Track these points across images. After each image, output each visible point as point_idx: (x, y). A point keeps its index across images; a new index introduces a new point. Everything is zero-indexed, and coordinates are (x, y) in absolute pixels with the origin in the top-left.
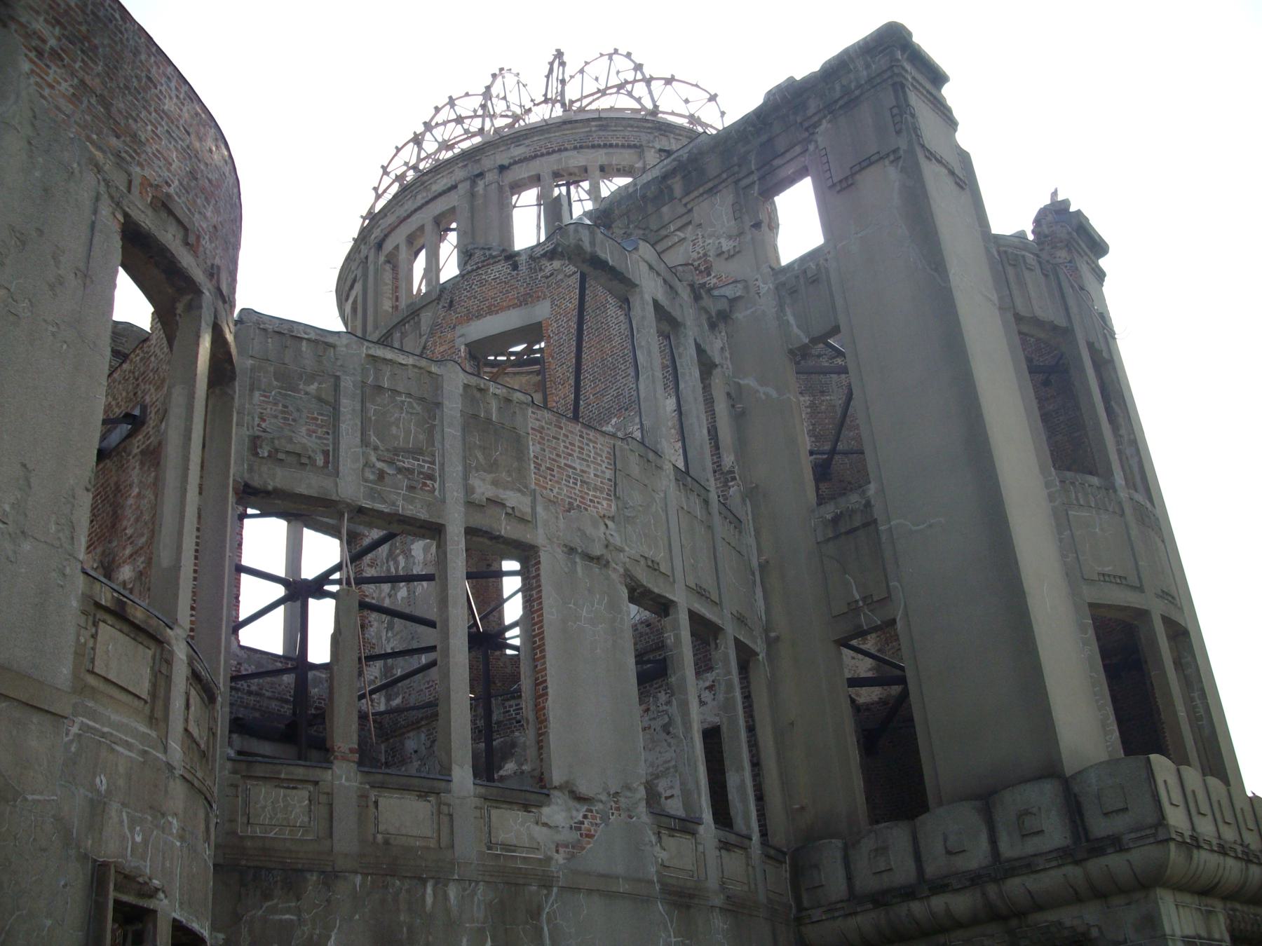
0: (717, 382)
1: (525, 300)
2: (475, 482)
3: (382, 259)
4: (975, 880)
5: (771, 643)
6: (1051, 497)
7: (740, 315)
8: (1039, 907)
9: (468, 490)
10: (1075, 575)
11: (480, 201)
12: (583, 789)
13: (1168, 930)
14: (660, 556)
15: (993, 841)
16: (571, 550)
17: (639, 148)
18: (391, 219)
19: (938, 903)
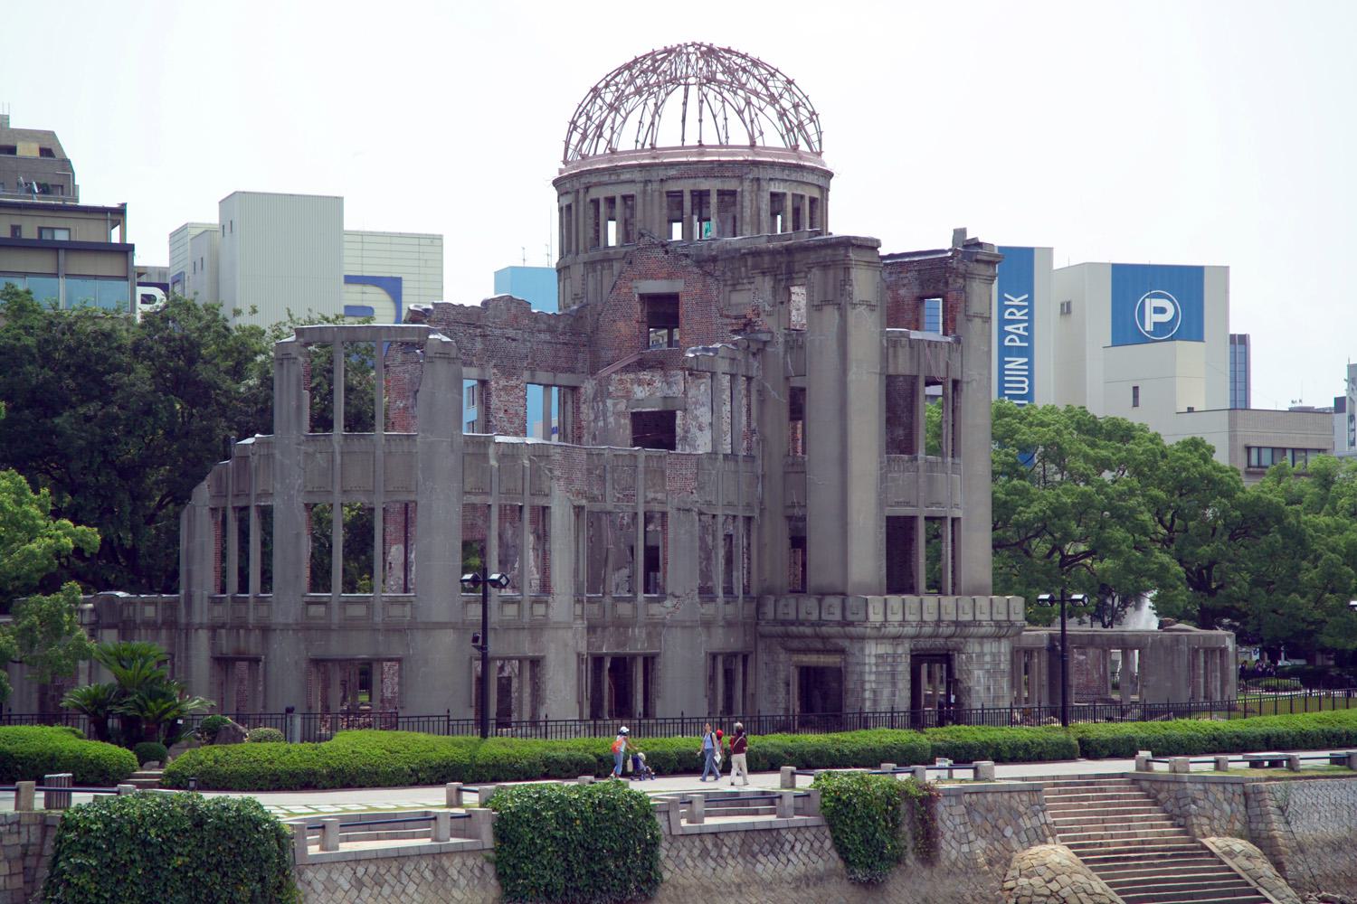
0: (754, 384)
1: (670, 276)
2: (648, 494)
3: (588, 200)
4: (813, 624)
5: (762, 511)
6: (881, 469)
7: (769, 349)
8: (835, 637)
9: (646, 497)
10: (882, 503)
11: (648, 198)
12: (677, 594)
13: (867, 652)
15: (820, 613)
16: (679, 509)
17: (741, 178)
18: (594, 179)
19: (801, 629)
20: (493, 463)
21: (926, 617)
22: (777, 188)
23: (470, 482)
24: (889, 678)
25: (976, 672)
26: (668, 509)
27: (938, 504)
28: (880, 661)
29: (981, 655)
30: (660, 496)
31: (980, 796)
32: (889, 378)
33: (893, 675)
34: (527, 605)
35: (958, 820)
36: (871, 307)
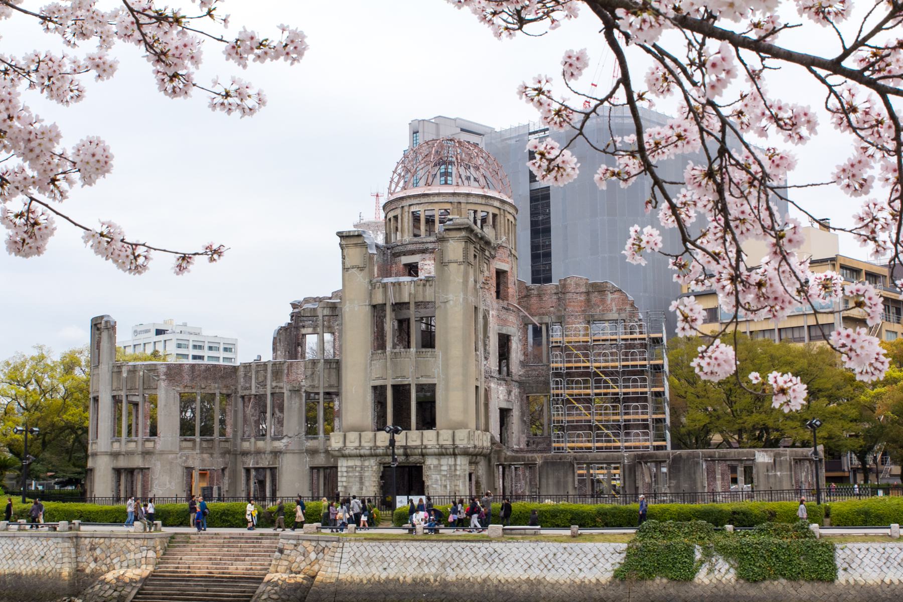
14: (316, 383)
20: (125, 375)
21: (379, 444)
22: (413, 209)
23: (115, 385)
24: (357, 479)
25: (434, 477)
26: (285, 391)
27: (404, 377)
28: (350, 469)
29: (438, 467)
30: (281, 384)
31: (107, 540)
32: (374, 307)
33: (361, 478)
34: (140, 443)
35: (59, 551)
36: (361, 269)
